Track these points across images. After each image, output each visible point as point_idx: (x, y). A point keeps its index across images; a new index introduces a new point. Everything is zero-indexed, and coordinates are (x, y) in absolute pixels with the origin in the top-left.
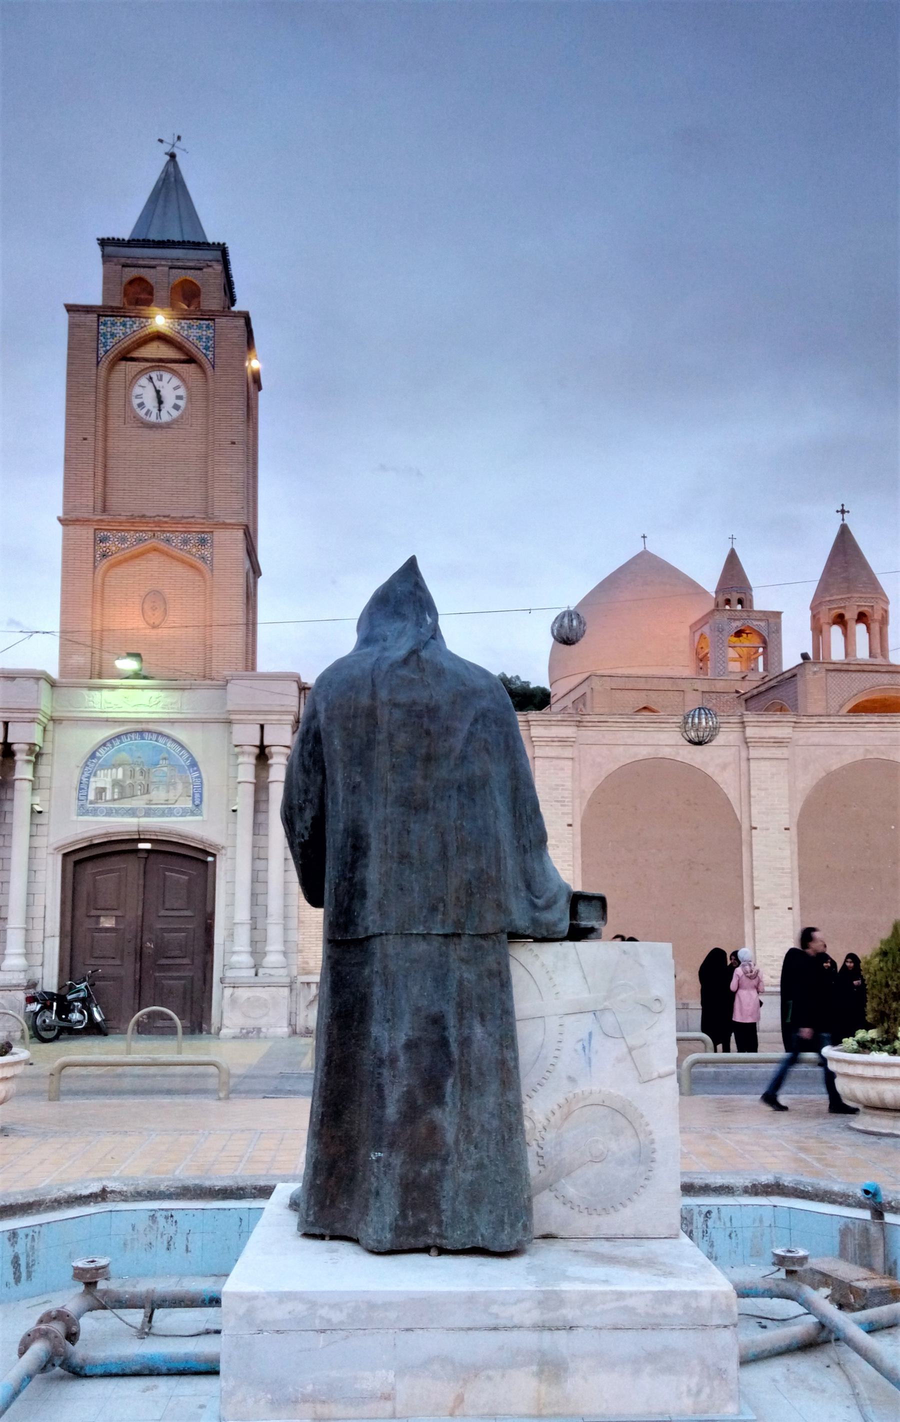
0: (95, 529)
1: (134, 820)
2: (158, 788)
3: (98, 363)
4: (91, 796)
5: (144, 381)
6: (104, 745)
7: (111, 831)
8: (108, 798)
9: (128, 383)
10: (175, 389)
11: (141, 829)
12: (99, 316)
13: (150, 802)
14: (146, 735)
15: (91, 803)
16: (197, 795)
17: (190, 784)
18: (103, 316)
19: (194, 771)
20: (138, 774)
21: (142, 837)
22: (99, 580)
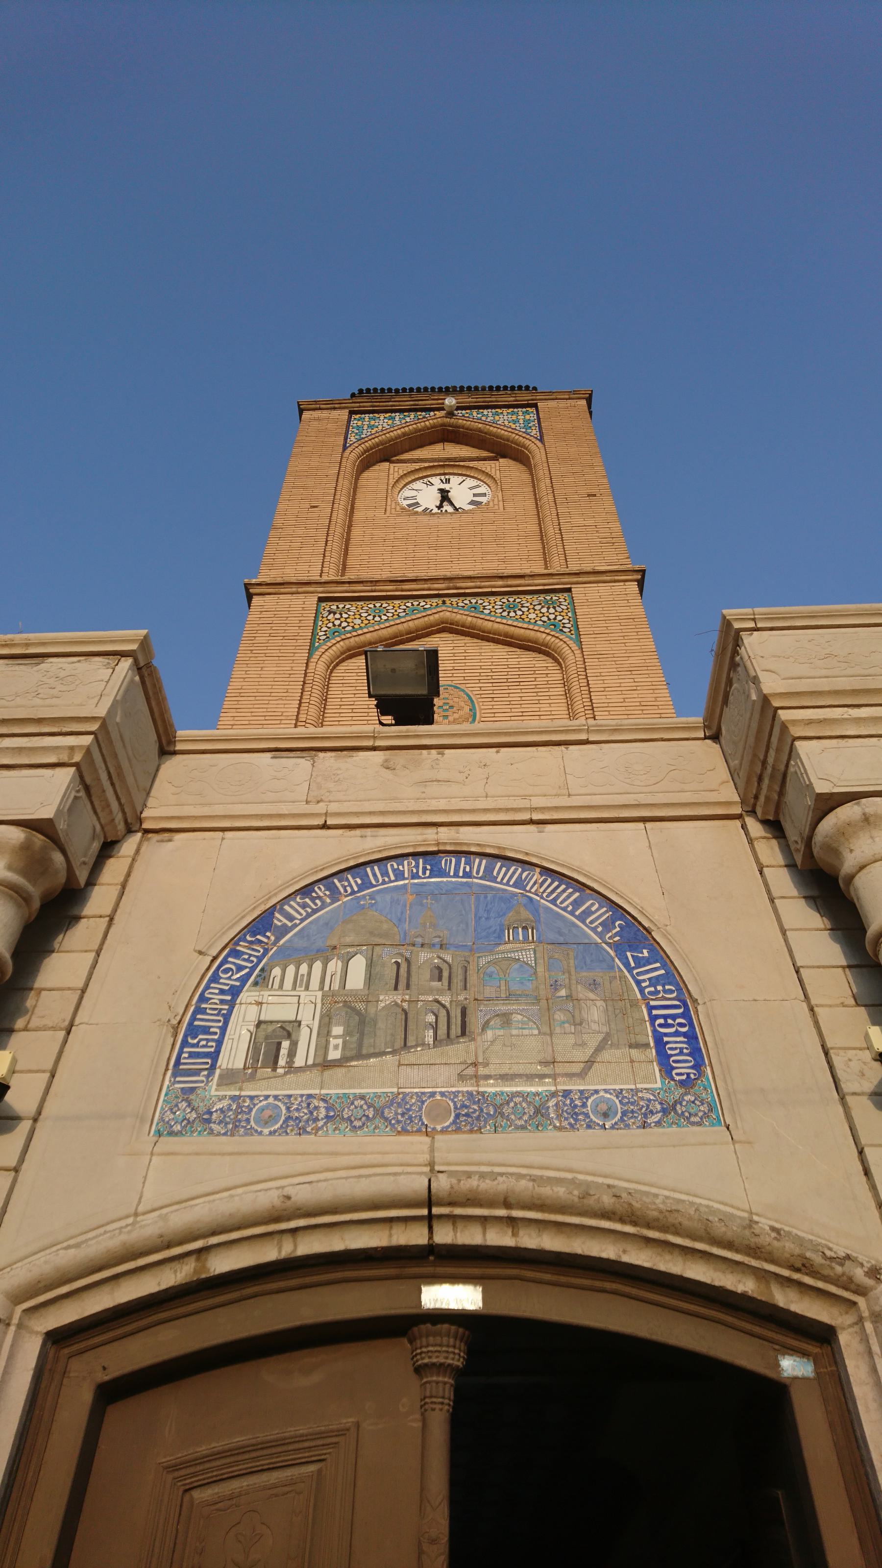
0: (321, 600)
1: (416, 1146)
2: (506, 1019)
3: (345, 448)
4: (235, 1053)
5: (418, 485)
6: (306, 890)
7: (302, 1195)
8: (299, 1061)
9: (392, 482)
10: (471, 488)
11: (442, 1184)
12: (351, 413)
13: (473, 1070)
14: (449, 863)
15: (230, 1078)
16: (676, 1044)
17: (634, 1004)
18: (356, 413)
19: (639, 962)
20: (422, 977)
21: (444, 1236)
22: (319, 667)
